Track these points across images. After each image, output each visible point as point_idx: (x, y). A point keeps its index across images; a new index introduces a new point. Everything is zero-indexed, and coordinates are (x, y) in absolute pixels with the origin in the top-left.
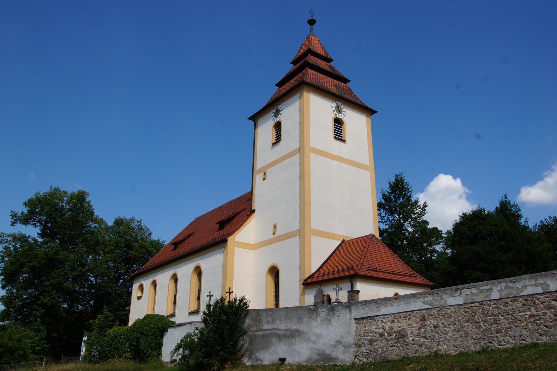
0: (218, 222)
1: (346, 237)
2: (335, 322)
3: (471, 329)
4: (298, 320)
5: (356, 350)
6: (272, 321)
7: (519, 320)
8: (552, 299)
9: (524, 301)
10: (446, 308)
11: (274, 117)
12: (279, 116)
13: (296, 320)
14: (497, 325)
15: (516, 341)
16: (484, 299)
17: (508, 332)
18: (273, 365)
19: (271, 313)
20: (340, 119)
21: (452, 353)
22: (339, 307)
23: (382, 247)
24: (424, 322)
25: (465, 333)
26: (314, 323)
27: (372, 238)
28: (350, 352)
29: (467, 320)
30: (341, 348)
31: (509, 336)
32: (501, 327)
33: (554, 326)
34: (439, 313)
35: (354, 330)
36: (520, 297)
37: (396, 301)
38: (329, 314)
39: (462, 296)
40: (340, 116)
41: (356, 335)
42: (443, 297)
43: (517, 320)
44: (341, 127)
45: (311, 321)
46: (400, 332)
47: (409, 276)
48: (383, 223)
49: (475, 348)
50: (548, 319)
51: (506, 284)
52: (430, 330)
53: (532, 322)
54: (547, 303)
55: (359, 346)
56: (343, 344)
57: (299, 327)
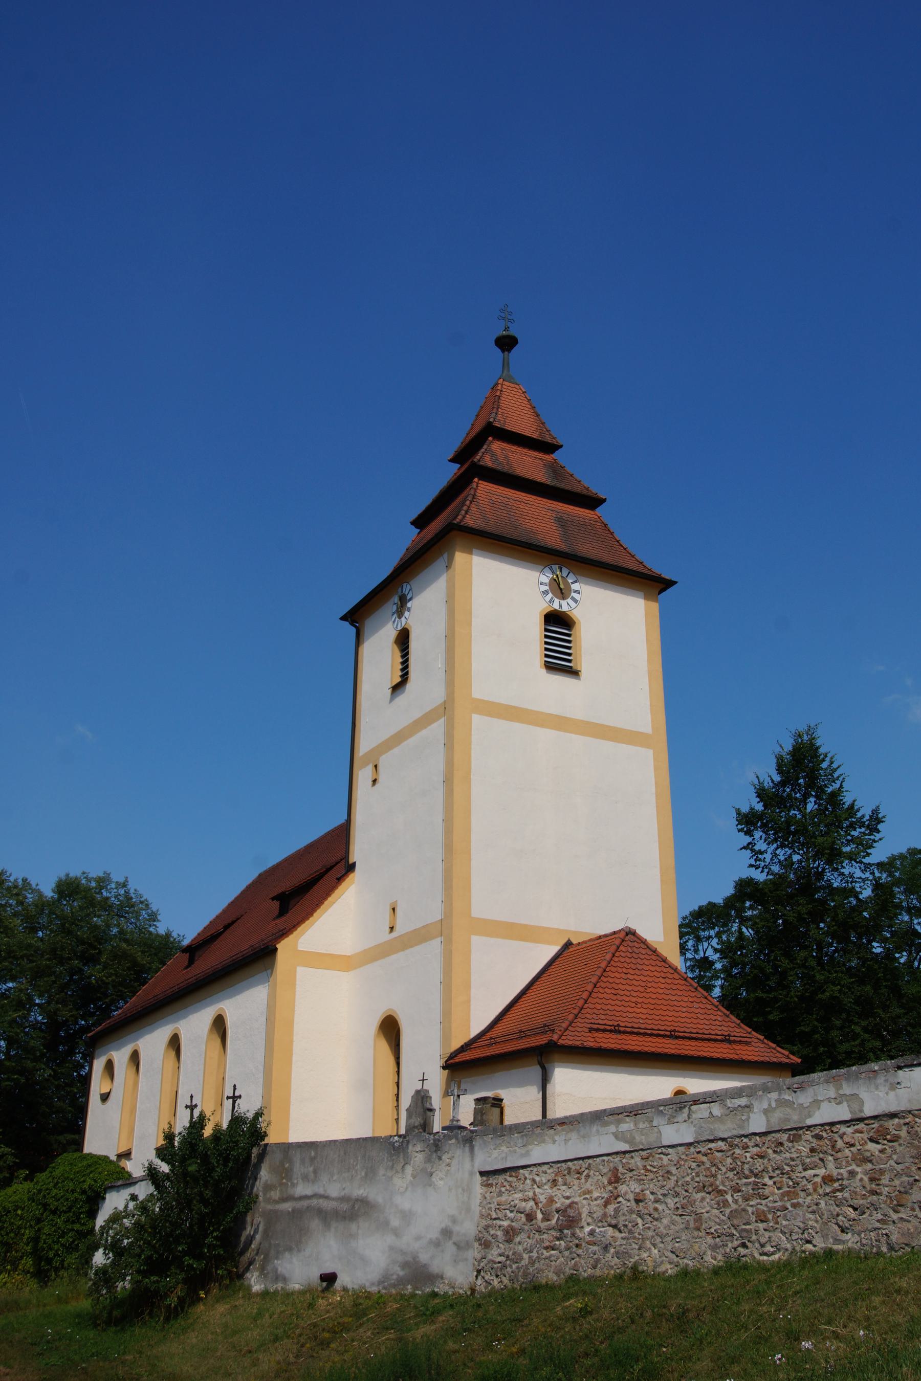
0: (274, 894)
1: (575, 933)
2: (441, 1179)
3: (708, 1208)
4: (366, 1174)
5: (479, 1256)
6: (312, 1175)
7: (802, 1191)
8: (869, 1136)
9: (814, 1140)
10: (660, 1151)
11: (395, 615)
12: (406, 614)
13: (363, 1174)
14: (759, 1201)
15: (794, 1243)
16: (735, 1133)
17: (779, 1219)
18: (308, 1290)
19: (313, 1154)
20: (564, 612)
21: (666, 1271)
22: (450, 1142)
23: (653, 963)
24: (616, 1188)
25: (694, 1219)
26: (399, 1182)
27: (627, 938)
28: (466, 1260)
29: (701, 1184)
30: (450, 1248)
31: (782, 1232)
32: (766, 1205)
33: (868, 1208)
34: (646, 1164)
35: (478, 1201)
36: (807, 1130)
37: (563, 1130)
38: (428, 1160)
39: (692, 1122)
40: (564, 606)
41: (482, 1216)
42: (655, 1123)
43: (798, 1189)
44: (569, 635)
45: (392, 1177)
46: (566, 1211)
47: (727, 1039)
48: (760, 869)
49: (715, 1259)
50: (858, 1190)
51: (780, 1094)
52: (626, 1209)
53: (827, 1194)
54: (859, 1148)
55: (486, 1245)
56: (455, 1238)
57: (367, 1191)
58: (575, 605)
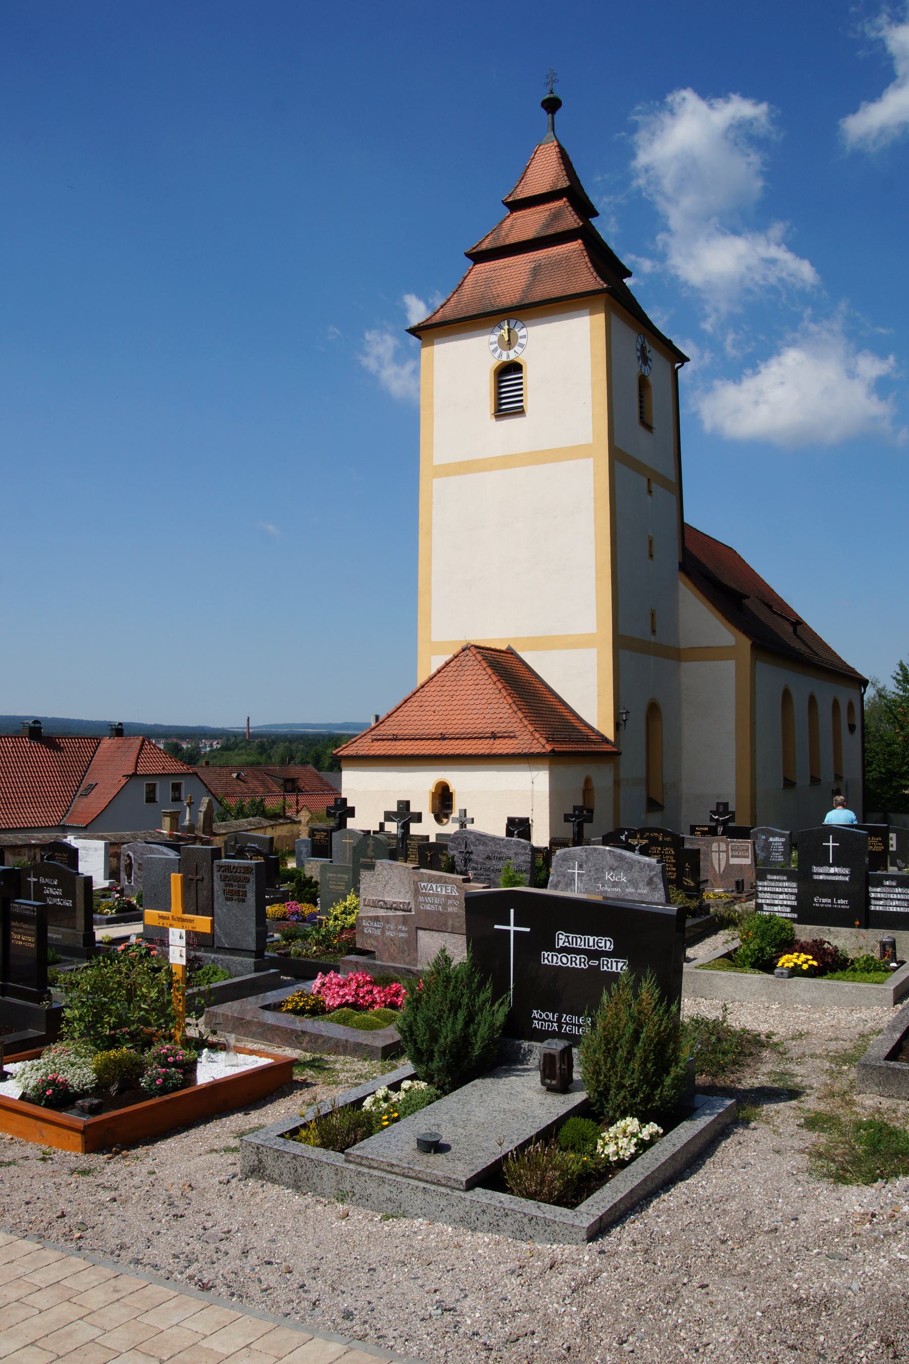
40: (511, 356)
58: (522, 349)
